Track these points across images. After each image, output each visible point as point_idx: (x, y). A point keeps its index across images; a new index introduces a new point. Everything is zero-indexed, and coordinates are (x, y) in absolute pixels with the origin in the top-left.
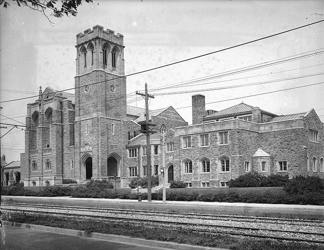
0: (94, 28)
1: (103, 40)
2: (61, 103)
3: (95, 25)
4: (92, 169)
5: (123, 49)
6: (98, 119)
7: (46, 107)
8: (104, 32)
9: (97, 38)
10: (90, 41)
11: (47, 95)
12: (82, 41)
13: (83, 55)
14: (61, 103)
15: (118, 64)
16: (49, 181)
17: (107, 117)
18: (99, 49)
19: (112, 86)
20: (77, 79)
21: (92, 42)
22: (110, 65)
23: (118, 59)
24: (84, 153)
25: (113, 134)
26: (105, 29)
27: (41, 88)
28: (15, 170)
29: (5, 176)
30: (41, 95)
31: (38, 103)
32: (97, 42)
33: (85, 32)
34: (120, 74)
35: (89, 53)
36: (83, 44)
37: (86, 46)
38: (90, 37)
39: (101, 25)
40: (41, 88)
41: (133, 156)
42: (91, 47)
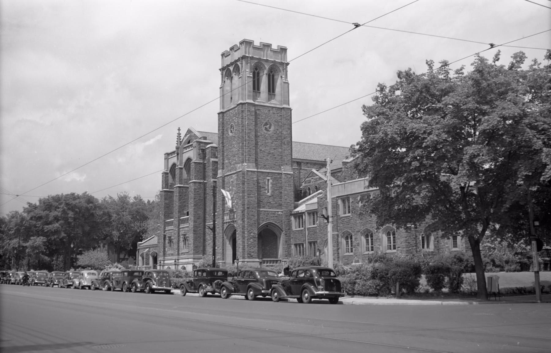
0: (241, 43)
1: (252, 58)
2: (203, 151)
3: (241, 39)
4: (480, 253)
5: (287, 67)
6: (243, 174)
7: (185, 157)
8: (256, 48)
9: (244, 57)
10: (236, 61)
11: (189, 140)
12: (228, 60)
13: (229, 81)
14: (203, 151)
15: (278, 90)
16: (185, 266)
17: (257, 169)
18: (246, 71)
19: (266, 124)
20: (221, 115)
21: (238, 63)
22: (263, 92)
23: (279, 83)
24: (228, 224)
25: (269, 194)
26: (257, 44)
27: (179, 130)
28: (152, 250)
29: (140, 258)
30: (179, 141)
31: (178, 152)
32: (244, 62)
33: (232, 49)
34: (281, 105)
35: (236, 78)
36: (228, 66)
37: (231, 68)
38: (237, 55)
39: (249, 38)
40: (179, 130)
41: (299, 227)
42: (237, 69)
